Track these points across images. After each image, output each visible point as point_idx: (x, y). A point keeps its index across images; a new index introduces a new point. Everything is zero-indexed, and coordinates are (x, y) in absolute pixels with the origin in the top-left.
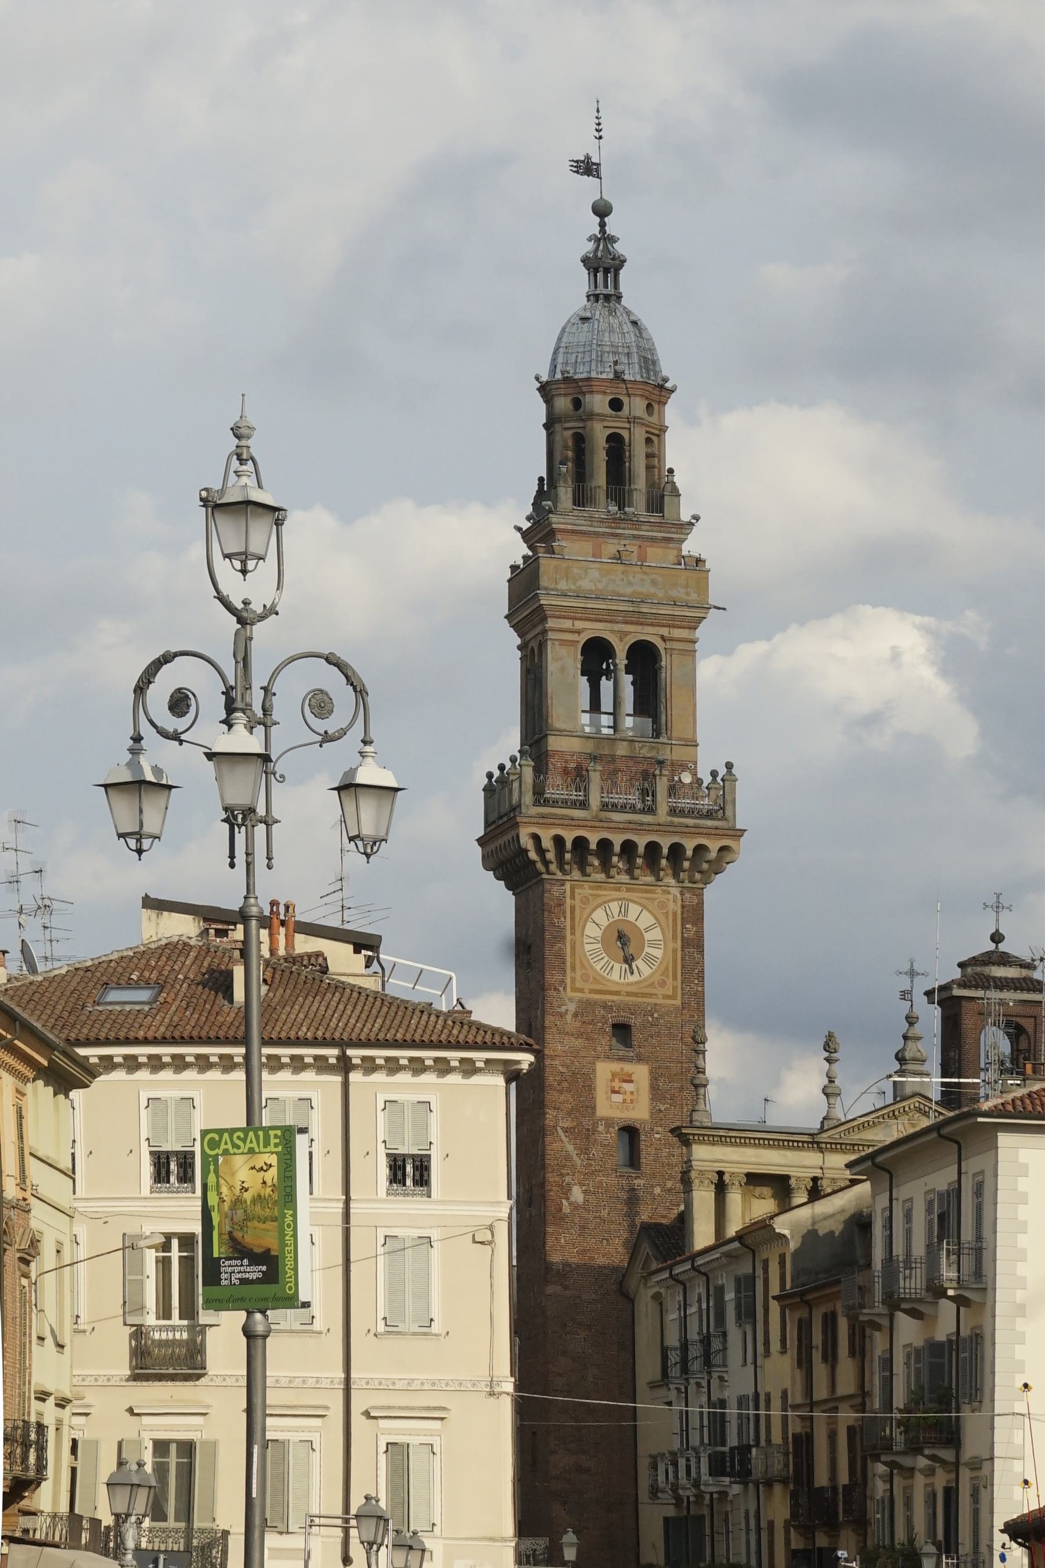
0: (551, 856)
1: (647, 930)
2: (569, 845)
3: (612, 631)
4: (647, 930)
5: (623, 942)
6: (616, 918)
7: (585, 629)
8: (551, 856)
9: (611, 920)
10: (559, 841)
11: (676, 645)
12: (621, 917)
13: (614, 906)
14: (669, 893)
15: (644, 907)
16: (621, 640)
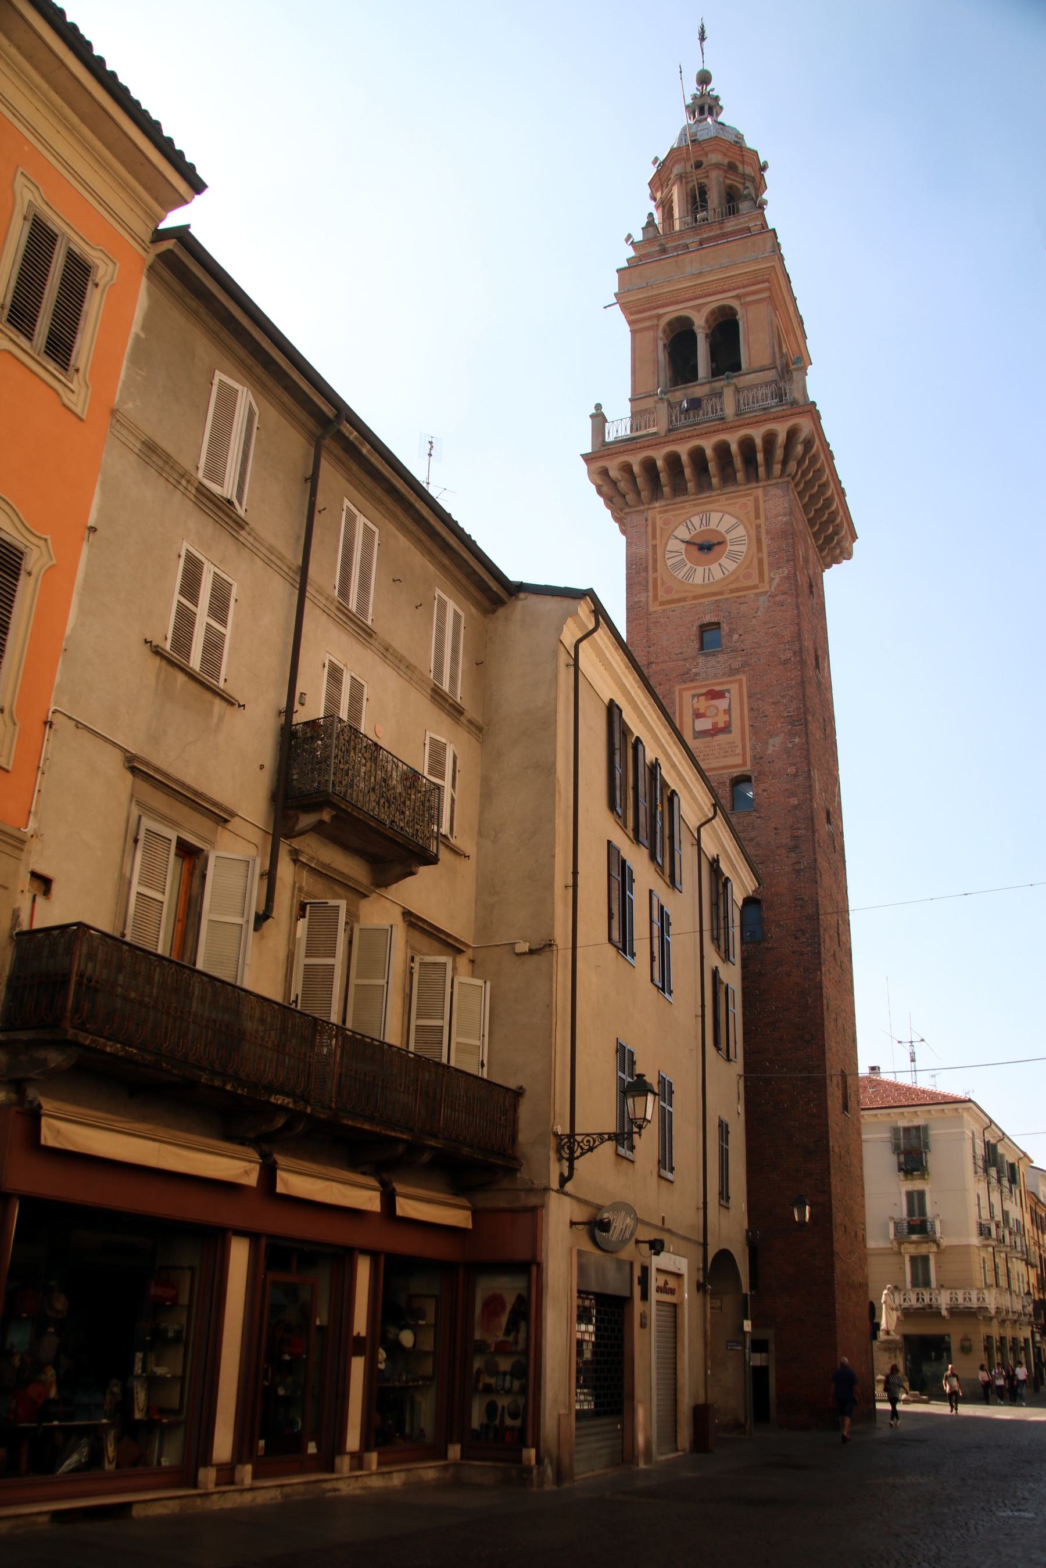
0: (623, 485)
1: (727, 532)
2: (636, 469)
3: (689, 308)
4: (727, 532)
5: (706, 547)
6: (698, 530)
7: (665, 314)
8: (623, 485)
9: (693, 533)
10: (627, 468)
11: (748, 299)
12: (703, 528)
13: (696, 520)
14: (750, 495)
15: (726, 512)
16: (699, 311)
